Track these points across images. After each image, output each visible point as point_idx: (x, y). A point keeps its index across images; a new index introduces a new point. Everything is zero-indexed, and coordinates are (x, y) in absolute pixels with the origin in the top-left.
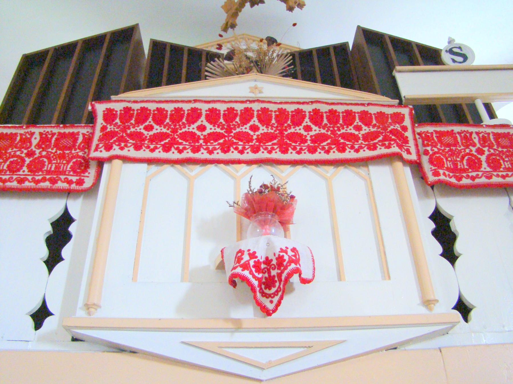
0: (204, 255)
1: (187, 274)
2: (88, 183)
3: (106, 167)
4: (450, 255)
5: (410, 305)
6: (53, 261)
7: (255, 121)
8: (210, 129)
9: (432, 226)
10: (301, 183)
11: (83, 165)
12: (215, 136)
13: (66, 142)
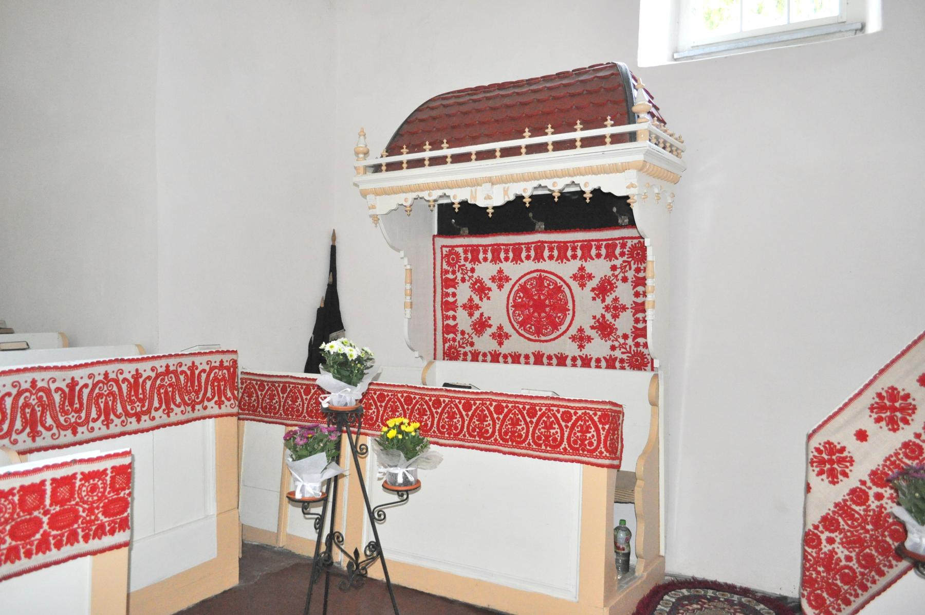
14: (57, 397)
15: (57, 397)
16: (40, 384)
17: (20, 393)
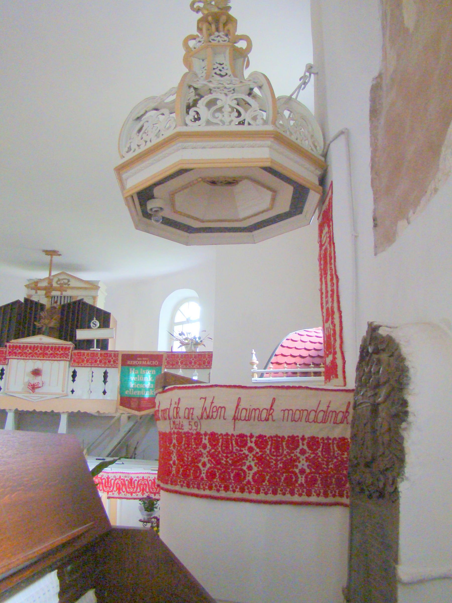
0: (27, 379)
2: (7, 363)
3: (10, 360)
4: (74, 381)
5: (60, 391)
7: (39, 349)
8: (30, 351)
9: (72, 374)
11: (5, 359)
12: (31, 353)
14: (127, 483)
15: (127, 483)
16: (122, 478)
17: (116, 479)
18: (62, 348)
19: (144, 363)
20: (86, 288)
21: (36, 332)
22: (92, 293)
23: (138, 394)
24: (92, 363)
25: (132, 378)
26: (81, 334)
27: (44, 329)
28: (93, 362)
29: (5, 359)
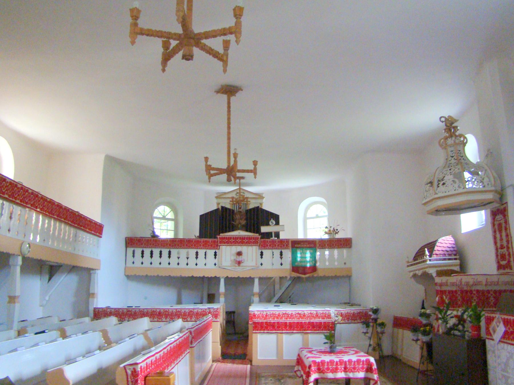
1: (231, 261)
4: (262, 258)
6: (215, 258)
10: (244, 249)
11: (217, 246)
13: (215, 242)
18: (254, 238)
19: (305, 246)
20: (255, 198)
21: (233, 228)
22: (259, 201)
23: (303, 264)
24: (273, 247)
25: (299, 255)
26: (264, 229)
27: (239, 226)
28: (273, 246)
29: (217, 246)
